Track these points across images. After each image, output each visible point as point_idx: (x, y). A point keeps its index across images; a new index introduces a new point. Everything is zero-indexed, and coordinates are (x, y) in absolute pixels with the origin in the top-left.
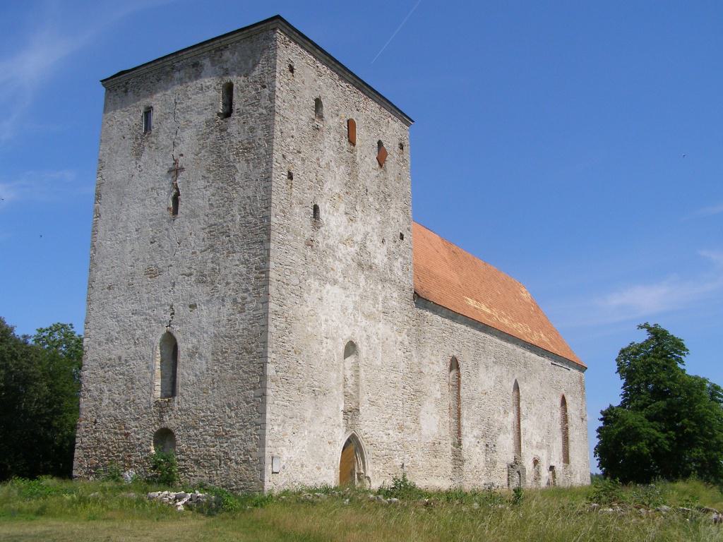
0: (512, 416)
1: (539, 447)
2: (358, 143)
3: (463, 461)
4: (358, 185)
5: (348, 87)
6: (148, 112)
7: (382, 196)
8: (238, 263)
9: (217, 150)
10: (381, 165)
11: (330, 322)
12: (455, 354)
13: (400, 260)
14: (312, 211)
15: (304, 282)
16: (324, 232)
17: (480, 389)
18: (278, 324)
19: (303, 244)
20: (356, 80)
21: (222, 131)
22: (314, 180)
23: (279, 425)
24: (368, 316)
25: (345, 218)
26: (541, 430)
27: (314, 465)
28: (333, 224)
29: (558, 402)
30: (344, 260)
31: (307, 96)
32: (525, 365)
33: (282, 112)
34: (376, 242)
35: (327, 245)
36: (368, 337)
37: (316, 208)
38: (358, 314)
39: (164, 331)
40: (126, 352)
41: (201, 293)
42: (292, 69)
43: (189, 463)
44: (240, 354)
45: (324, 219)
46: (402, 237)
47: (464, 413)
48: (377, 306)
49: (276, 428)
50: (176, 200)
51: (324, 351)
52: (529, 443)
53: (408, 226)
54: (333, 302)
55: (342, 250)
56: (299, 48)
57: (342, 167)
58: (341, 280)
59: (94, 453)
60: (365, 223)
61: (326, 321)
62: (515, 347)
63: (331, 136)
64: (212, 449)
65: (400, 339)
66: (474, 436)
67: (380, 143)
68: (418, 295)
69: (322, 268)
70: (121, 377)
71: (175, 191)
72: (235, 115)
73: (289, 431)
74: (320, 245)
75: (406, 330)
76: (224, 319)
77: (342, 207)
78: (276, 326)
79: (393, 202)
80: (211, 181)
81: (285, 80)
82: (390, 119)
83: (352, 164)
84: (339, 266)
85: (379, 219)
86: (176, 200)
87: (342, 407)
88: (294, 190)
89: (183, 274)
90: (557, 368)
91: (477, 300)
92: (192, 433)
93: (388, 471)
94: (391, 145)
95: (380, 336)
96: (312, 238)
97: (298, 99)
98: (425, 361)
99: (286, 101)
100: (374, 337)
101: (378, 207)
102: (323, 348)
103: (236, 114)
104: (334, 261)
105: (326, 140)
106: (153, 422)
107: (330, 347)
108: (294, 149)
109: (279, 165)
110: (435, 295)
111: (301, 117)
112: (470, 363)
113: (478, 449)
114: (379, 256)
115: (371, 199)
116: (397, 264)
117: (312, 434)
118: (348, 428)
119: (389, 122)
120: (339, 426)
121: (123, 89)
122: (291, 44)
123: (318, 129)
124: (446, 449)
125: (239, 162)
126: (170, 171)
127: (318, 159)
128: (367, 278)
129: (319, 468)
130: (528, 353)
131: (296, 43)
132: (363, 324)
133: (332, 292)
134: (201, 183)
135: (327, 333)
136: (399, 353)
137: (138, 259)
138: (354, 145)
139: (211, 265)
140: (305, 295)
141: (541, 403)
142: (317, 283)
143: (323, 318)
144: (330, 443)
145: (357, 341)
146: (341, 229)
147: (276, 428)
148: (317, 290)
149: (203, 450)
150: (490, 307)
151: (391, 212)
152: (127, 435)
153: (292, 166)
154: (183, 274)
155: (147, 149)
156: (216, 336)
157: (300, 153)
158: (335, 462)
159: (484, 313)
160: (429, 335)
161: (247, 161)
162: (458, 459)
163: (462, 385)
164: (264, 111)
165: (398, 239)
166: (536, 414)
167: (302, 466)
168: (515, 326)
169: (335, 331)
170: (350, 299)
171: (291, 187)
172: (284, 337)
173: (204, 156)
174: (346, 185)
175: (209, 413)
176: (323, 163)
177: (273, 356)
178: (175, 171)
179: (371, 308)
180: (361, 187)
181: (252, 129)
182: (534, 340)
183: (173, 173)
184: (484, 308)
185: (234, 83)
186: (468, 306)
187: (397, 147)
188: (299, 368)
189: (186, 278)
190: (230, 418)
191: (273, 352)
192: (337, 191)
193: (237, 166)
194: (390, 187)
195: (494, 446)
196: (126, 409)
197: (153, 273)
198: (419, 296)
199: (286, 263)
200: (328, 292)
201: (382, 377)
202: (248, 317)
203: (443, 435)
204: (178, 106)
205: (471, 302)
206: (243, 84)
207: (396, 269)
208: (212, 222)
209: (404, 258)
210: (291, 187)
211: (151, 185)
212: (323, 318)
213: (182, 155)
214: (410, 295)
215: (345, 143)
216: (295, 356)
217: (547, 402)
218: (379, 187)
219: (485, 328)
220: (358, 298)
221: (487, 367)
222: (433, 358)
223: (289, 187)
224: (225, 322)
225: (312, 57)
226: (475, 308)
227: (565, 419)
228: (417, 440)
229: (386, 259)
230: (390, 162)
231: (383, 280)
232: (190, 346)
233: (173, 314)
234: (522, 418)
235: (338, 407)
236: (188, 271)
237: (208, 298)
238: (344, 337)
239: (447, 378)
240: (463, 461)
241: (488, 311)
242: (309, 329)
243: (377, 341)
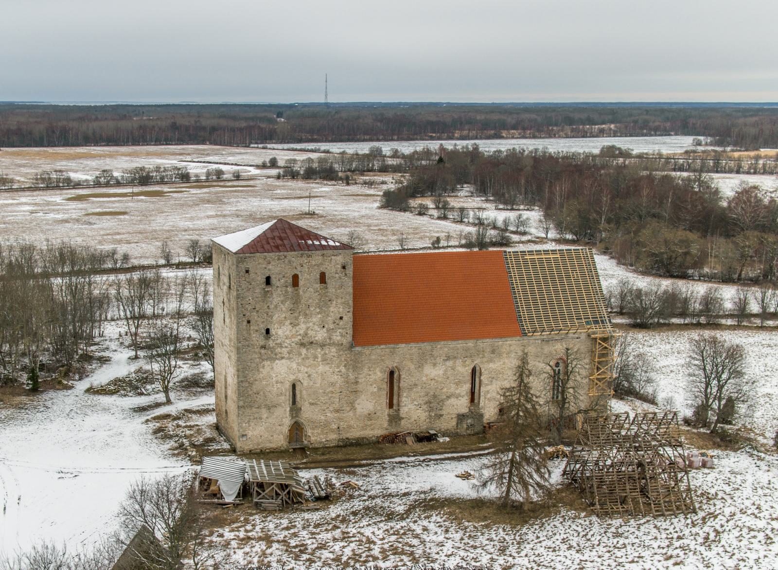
14: (265, 332)
24: (308, 367)
28: (280, 332)
35: (276, 344)
46: (341, 318)
84: (285, 350)
98: (361, 376)
128: (307, 349)
140: (261, 370)
143: (274, 375)
146: (288, 332)
151: (332, 309)
192: (284, 315)
212: (274, 375)
215: (290, 289)
235: (285, 410)
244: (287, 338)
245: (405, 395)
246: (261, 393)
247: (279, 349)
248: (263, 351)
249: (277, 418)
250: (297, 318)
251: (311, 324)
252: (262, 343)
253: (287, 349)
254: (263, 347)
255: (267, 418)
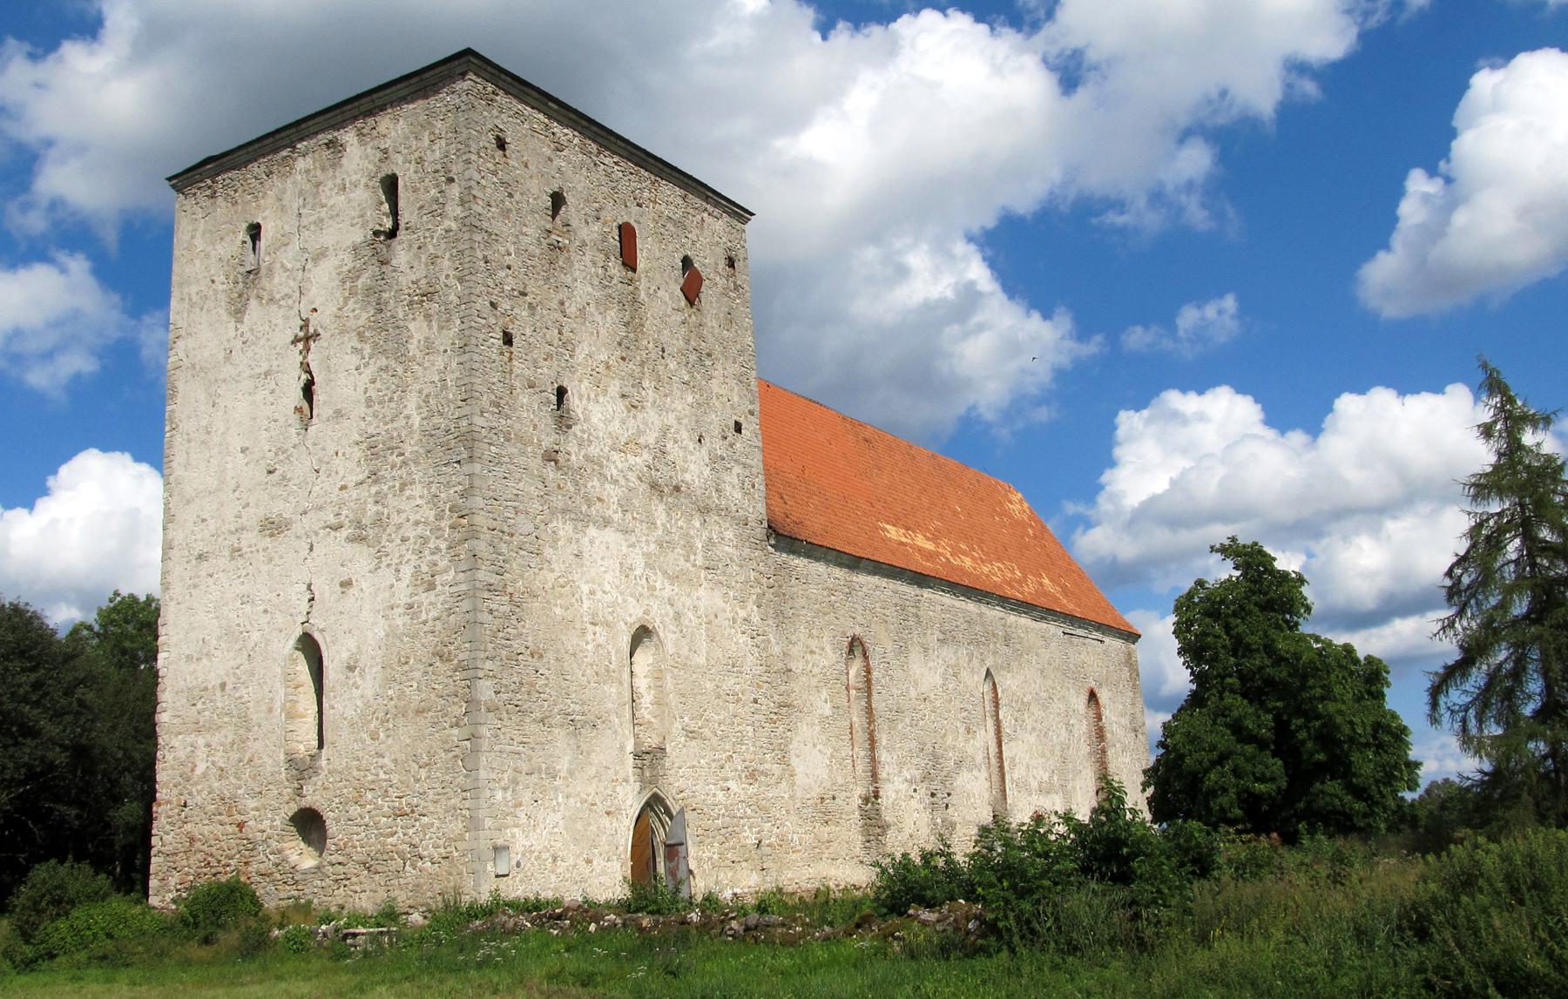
0: (986, 736)
1: (1046, 789)
2: (641, 264)
3: (884, 828)
4: (645, 342)
5: (616, 163)
6: (255, 231)
7: (693, 357)
8: (419, 502)
9: (375, 298)
10: (691, 304)
11: (599, 595)
12: (858, 631)
13: (737, 469)
14: (554, 399)
15: (542, 526)
16: (579, 434)
17: (913, 694)
18: (494, 606)
19: (539, 460)
20: (634, 150)
21: (382, 263)
22: (556, 342)
23: (505, 789)
24: (674, 578)
25: (621, 405)
26: (1048, 759)
27: (578, 856)
28: (596, 418)
29: (1080, 702)
30: (622, 482)
31: (535, 191)
32: (1007, 640)
33: (485, 225)
34: (684, 443)
35: (587, 457)
36: (678, 616)
37: (561, 393)
38: (656, 574)
39: (299, 632)
40: (234, 673)
41: (360, 561)
42: (501, 144)
43: (351, 868)
44: (431, 665)
45: (579, 411)
46: (738, 428)
47: (883, 739)
48: (692, 557)
49: (499, 795)
50: (308, 391)
51: (589, 647)
52: (1023, 786)
53: (750, 407)
54: (603, 559)
55: (617, 464)
56: (515, 102)
57: (612, 314)
58: (616, 517)
59: (185, 862)
60: (661, 409)
61: (592, 593)
62: (984, 608)
63: (588, 258)
64: (390, 840)
65: (742, 614)
66: (906, 780)
67: (687, 262)
68: (775, 531)
69: (578, 499)
70: (226, 719)
71: (304, 377)
72: (402, 234)
73: (526, 797)
74: (573, 458)
75: (755, 597)
76: (403, 597)
77: (615, 387)
78: (491, 611)
79: (718, 366)
80: (367, 356)
81: (489, 165)
82: (705, 215)
83: (632, 305)
84: (613, 493)
85: (690, 399)
86: (308, 391)
87: (630, 747)
88: (515, 363)
89: (327, 527)
90: (1075, 640)
91: (907, 529)
92: (355, 810)
93: (729, 856)
94: (708, 263)
95: (701, 611)
96: (556, 448)
97: (517, 196)
99: (493, 203)
100: (690, 614)
101: (686, 378)
102: (587, 643)
103: (404, 232)
104: (602, 485)
105: (577, 266)
106: (287, 798)
107: (602, 640)
108: (513, 289)
109: (484, 321)
110: (814, 526)
111: (525, 229)
112: (890, 646)
113: (914, 803)
114: (692, 467)
115: (672, 366)
116: (731, 479)
117: (572, 800)
118: (644, 783)
119: (703, 220)
120: (626, 781)
121: (208, 192)
122: (498, 98)
123: (560, 248)
124: (847, 808)
125: (414, 319)
126: (296, 341)
127: (562, 303)
128: (669, 511)
129: (589, 862)
130: (1012, 618)
131: (507, 93)
132: (667, 592)
133: (603, 545)
134: (354, 360)
135: (594, 615)
136: (743, 639)
137: (248, 505)
138: (634, 270)
139: (375, 509)
141: (1045, 707)
142: (569, 527)
143: (585, 588)
144: (608, 813)
145: (655, 622)
146: (615, 426)
147: (499, 795)
148: (570, 541)
149: (373, 845)
150: (934, 539)
152: (241, 826)
153: (511, 321)
154: (327, 527)
155: (253, 303)
156: (387, 635)
157: (524, 294)
158: (621, 848)
159: (920, 550)
160: (802, 602)
161: (428, 317)
162: (873, 821)
163: (875, 688)
164: (454, 226)
165: (731, 433)
166: (1034, 729)
167: (555, 859)
168: (986, 569)
169: (610, 610)
170: (637, 550)
171: (511, 359)
172: (509, 630)
173: (353, 311)
174: (620, 344)
175: (382, 776)
176: (572, 309)
177: (488, 665)
178: (307, 338)
179: (682, 562)
180: (651, 345)
181: (434, 259)
182: (1027, 591)
183: (300, 346)
184: (920, 541)
185: (399, 174)
186: (885, 540)
187: (722, 264)
188: (540, 683)
189: (333, 533)
190: (418, 781)
191: (487, 658)
192: (603, 357)
193: (411, 326)
194: (711, 339)
195: (949, 794)
196: (239, 779)
197: (273, 527)
198: (778, 534)
199: (505, 497)
200: (592, 542)
201: (709, 685)
202: (441, 598)
203: (840, 780)
204: (305, 221)
205: (893, 533)
206: (415, 177)
207: (728, 488)
208: (371, 430)
209: (745, 466)
210: (511, 359)
211: (264, 367)
212: (585, 588)
213: (315, 310)
214: (760, 531)
215: (615, 268)
216: (534, 662)
217: (1057, 706)
218: (688, 342)
219: (921, 579)
220: (652, 546)
221: (926, 650)
222: (813, 644)
223: (506, 359)
224: (401, 610)
225: (541, 116)
226: (902, 543)
227: (1100, 734)
228: (786, 796)
229: (707, 472)
230: (708, 294)
231: (704, 510)
232: (345, 655)
233: (313, 599)
234: (1005, 740)
235: (622, 748)
236: (332, 520)
237: (372, 567)
238: (628, 619)
239: (844, 678)
240: (884, 828)
241: (930, 546)
242: (558, 611)
243: (695, 621)
244: (613, 449)
245: (884, 742)
246: (550, 656)
247: (596, 483)
248: (550, 473)
249: (597, 776)
250: (638, 385)
251: (671, 419)
252: (548, 442)
253: (619, 491)
254: (551, 457)
255: (571, 773)
